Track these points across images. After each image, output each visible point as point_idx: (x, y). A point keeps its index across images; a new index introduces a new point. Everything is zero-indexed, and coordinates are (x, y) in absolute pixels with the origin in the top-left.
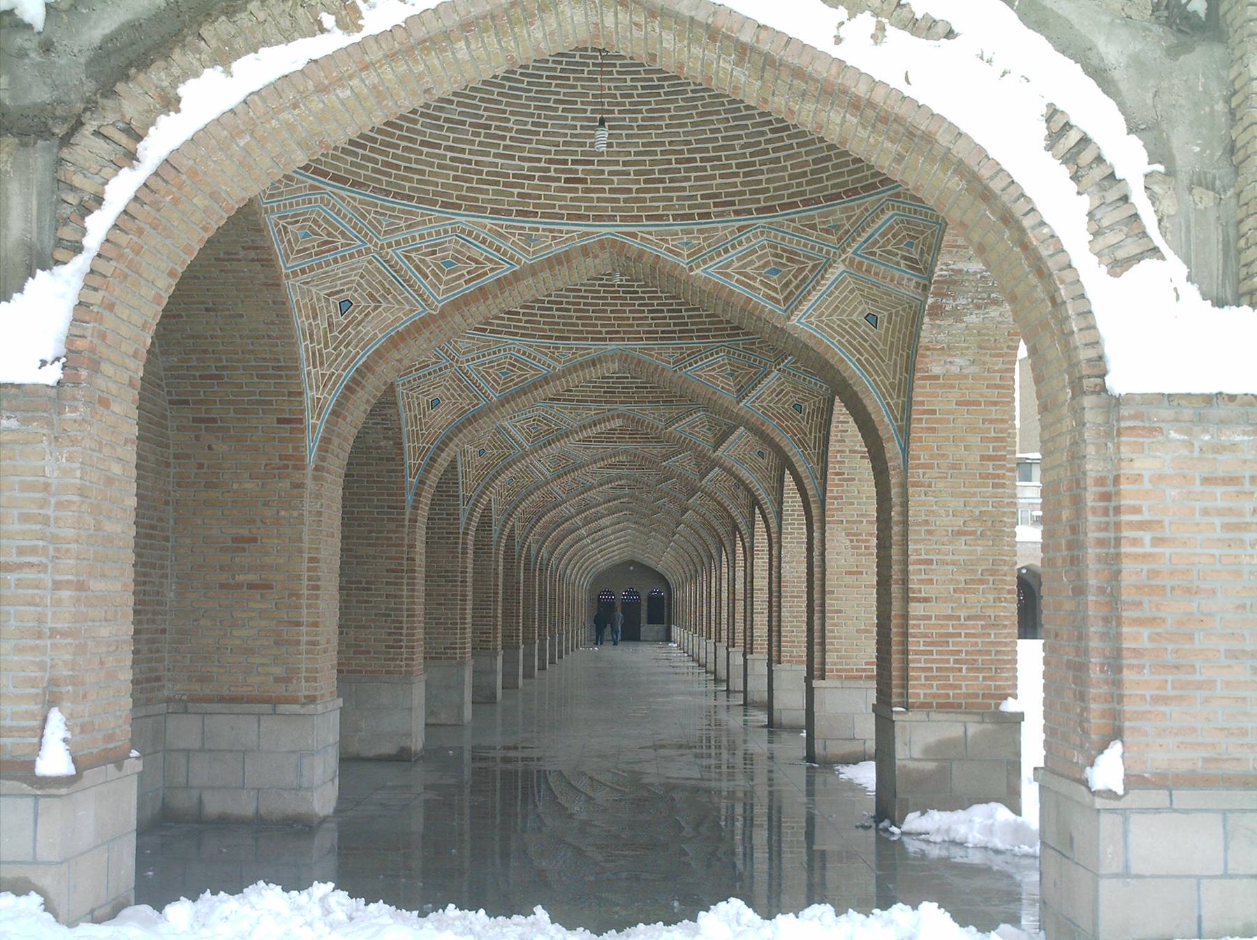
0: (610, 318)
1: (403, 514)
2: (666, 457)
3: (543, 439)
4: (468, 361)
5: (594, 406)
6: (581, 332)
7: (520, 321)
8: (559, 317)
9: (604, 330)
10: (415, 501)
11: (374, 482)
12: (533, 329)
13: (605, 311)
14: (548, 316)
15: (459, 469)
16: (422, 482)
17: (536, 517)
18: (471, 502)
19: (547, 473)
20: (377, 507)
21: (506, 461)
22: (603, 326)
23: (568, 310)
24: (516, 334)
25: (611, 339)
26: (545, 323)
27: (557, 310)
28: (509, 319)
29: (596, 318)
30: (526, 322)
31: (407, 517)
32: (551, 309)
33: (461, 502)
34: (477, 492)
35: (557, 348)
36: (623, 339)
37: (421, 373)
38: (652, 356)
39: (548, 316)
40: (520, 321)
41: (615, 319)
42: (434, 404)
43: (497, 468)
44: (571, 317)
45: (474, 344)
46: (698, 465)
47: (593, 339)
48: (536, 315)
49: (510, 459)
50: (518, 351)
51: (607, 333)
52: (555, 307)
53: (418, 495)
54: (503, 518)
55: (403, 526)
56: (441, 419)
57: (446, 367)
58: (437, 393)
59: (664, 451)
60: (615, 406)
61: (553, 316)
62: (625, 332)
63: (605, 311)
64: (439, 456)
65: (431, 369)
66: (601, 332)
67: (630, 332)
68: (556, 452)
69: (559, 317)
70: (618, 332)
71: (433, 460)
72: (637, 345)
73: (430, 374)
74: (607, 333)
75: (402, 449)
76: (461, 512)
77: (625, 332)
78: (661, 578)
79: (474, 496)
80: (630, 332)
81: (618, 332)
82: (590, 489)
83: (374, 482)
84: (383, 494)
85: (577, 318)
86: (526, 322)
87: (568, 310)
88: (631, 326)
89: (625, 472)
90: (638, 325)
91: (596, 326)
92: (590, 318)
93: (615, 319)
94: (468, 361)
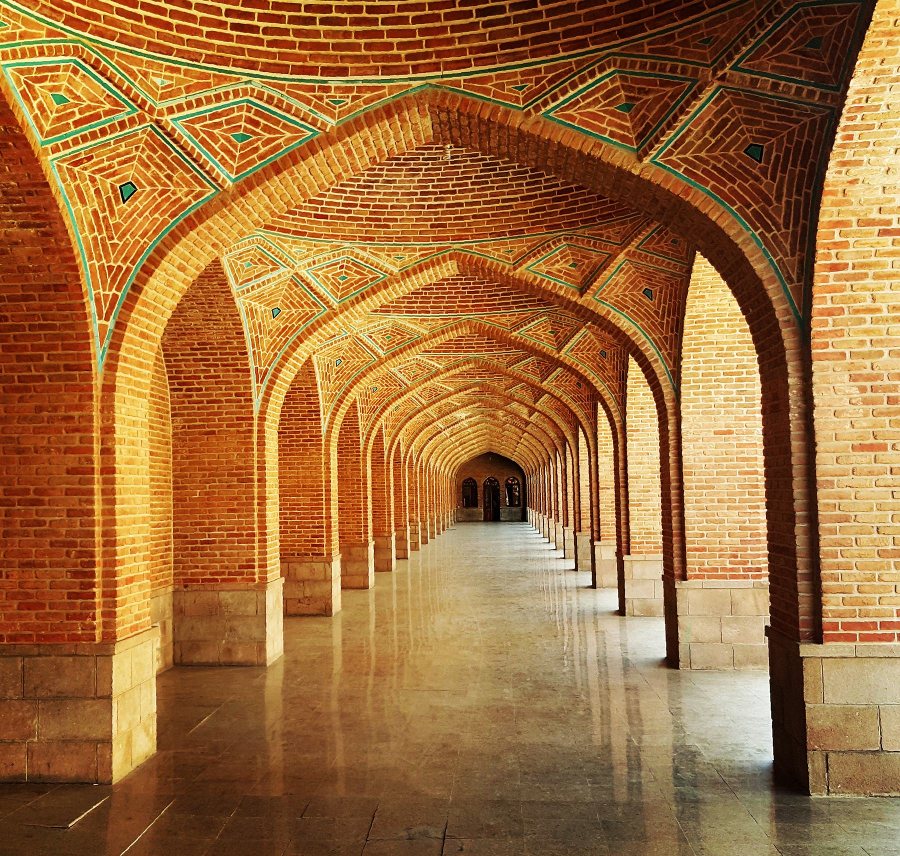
0: (412, 33)
1: (89, 378)
2: (516, 326)
3: (354, 293)
4: (171, 110)
5: (418, 245)
6: (365, 59)
7: (260, 42)
8: (327, 34)
9: (403, 53)
10: (110, 356)
11: (42, 327)
12: (282, 56)
13: (404, 20)
14: (307, 34)
15: (247, 336)
16: (120, 325)
17: (380, 408)
18: (269, 376)
19: (380, 352)
20: (48, 368)
21: (309, 323)
22: (401, 46)
23: (342, 22)
24: (252, 65)
25: (416, 69)
26: (303, 46)
27: (323, 22)
28: (240, 39)
29: (391, 34)
30: (271, 44)
31: (98, 382)
32: (312, 21)
33: (253, 378)
34: (275, 365)
35: (327, 89)
36: (436, 67)
37: (86, 129)
38: (487, 91)
39: (307, 34)
40: (260, 42)
41: (423, 32)
42: (127, 191)
43: (298, 333)
44: (347, 34)
45: (180, 82)
46: (555, 332)
47: (386, 70)
48: (286, 32)
49: (313, 321)
50: (260, 96)
51: (409, 57)
52: (319, 16)
53: (115, 346)
54: (333, 405)
55: (91, 397)
56: (141, 218)
57: (132, 121)
58: (130, 173)
59: (514, 319)
60: (445, 244)
61: (317, 34)
62: (439, 54)
63: (404, 20)
64: (145, 282)
65: (105, 122)
66: (398, 58)
67: (449, 53)
68: (388, 327)
69: (327, 34)
70: (427, 55)
71: (137, 289)
72: (459, 76)
73: (103, 132)
74: (409, 57)
75: (75, 268)
76: (254, 391)
77: (439, 54)
78: (513, 466)
79: (271, 371)
80: (449, 53)
81: (427, 55)
82: (437, 374)
83: (42, 327)
84: (55, 347)
85: (358, 35)
86: (271, 44)
87: (342, 22)
88: (450, 41)
89: (472, 355)
90: (461, 40)
91: (390, 46)
92: (380, 34)
93: (423, 32)
94: (171, 110)
